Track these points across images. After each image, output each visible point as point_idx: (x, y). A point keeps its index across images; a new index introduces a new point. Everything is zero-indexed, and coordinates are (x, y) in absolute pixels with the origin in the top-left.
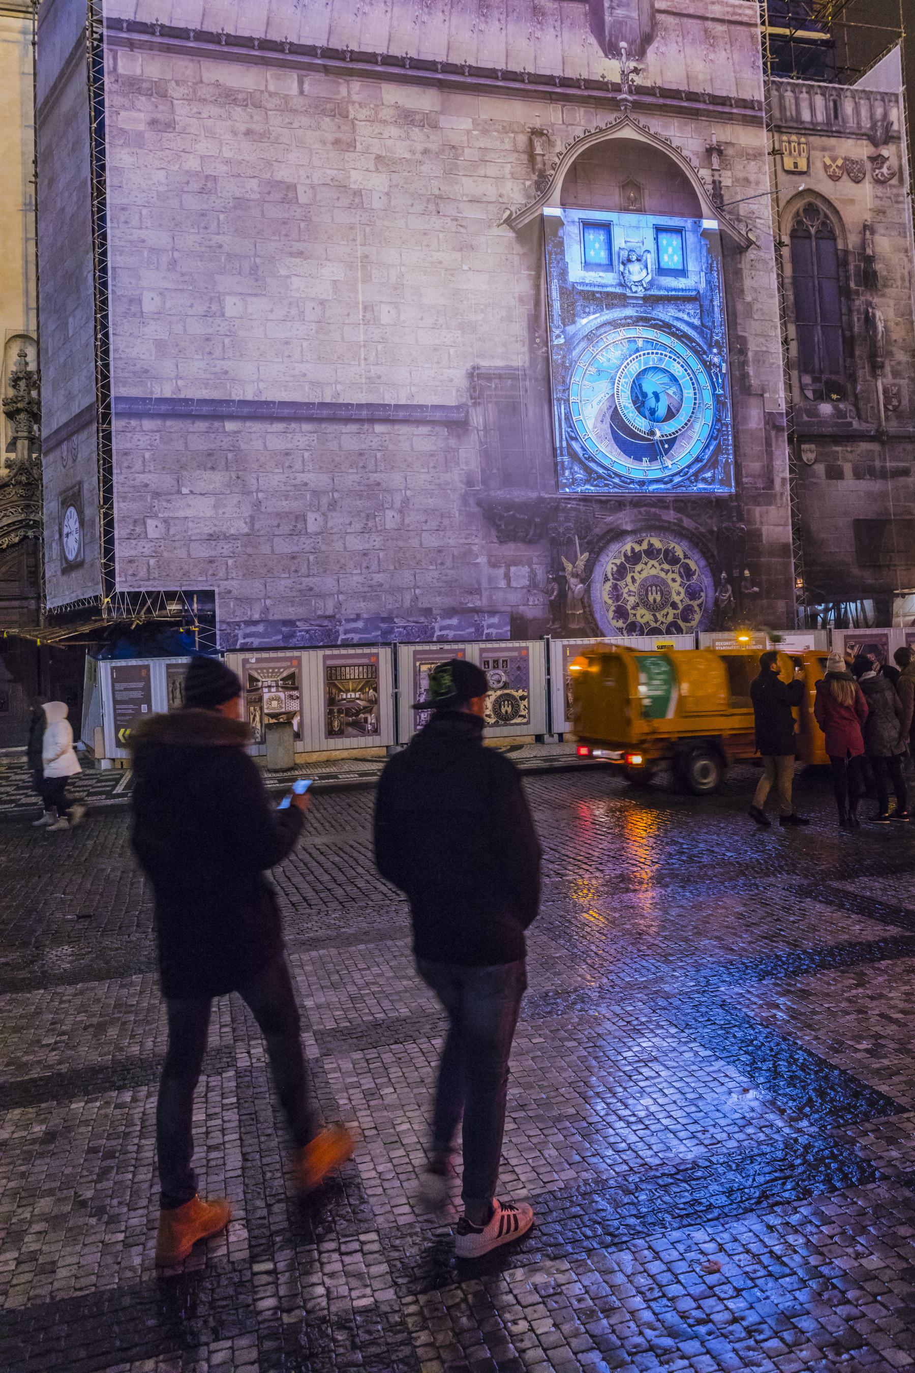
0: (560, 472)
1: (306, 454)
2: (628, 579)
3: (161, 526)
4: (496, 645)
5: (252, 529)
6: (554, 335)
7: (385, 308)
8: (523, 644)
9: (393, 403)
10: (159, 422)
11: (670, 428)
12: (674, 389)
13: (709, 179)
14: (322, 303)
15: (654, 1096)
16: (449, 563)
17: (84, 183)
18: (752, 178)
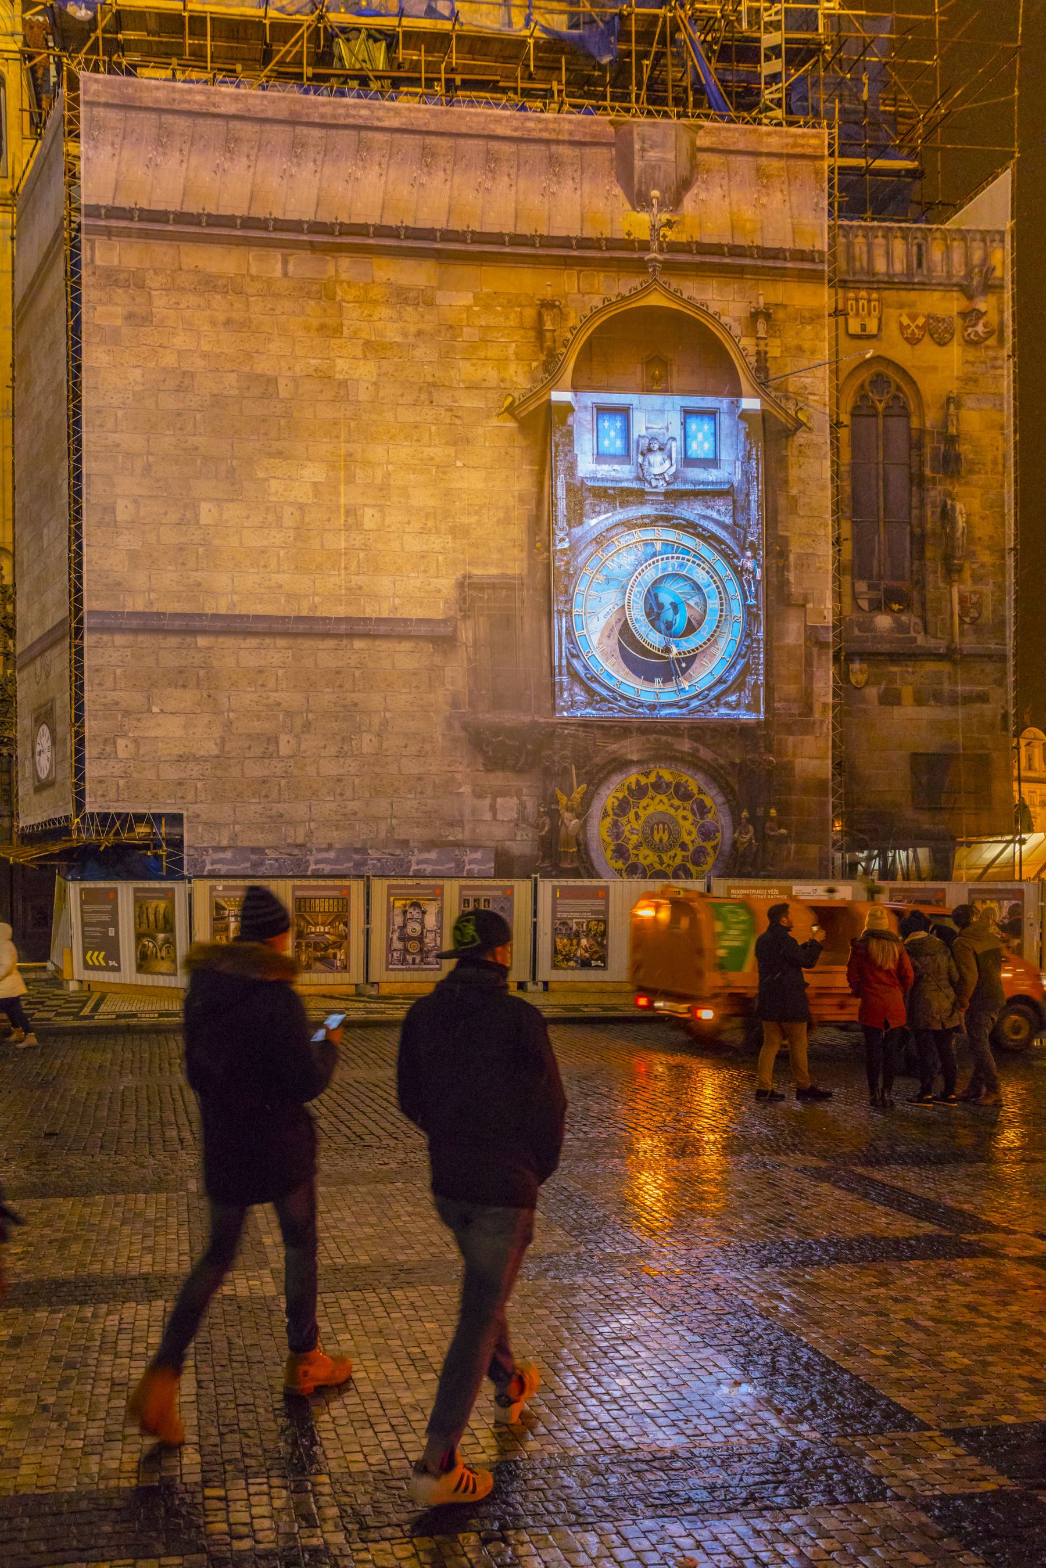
0: (557, 693)
1: (280, 672)
2: (631, 815)
3: (131, 746)
4: (478, 883)
5: (222, 750)
6: (558, 538)
7: (369, 512)
8: (506, 883)
9: (374, 616)
10: (131, 637)
11: (689, 644)
12: (696, 599)
13: (752, 350)
14: (301, 507)
16: (429, 791)
17: (60, 385)
18: (806, 345)
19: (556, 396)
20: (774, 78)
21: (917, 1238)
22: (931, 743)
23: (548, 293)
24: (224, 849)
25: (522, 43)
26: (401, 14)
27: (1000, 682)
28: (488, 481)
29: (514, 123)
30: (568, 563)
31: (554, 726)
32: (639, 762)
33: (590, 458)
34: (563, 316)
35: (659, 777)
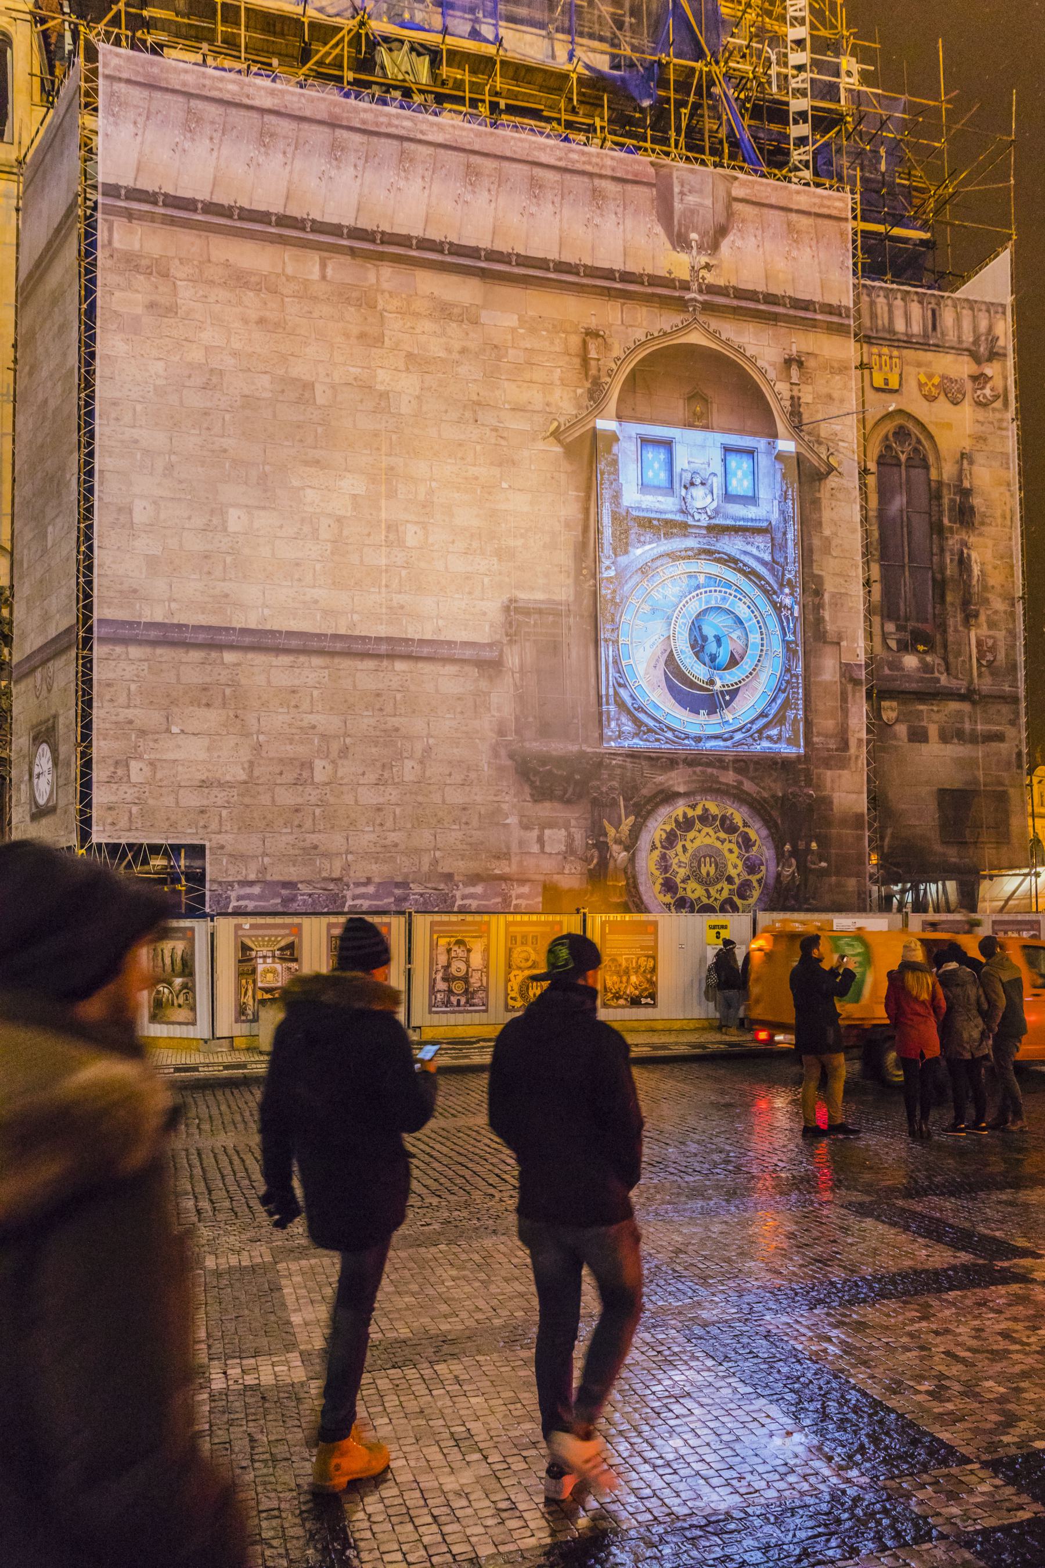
0: (605, 723)
1: (316, 693)
5: (251, 777)
6: (604, 566)
10: (148, 650)
11: (732, 677)
12: (738, 633)
13: (786, 395)
15: (685, 1437)
16: (475, 822)
19: (601, 424)
20: (802, 141)
21: (954, 1268)
22: (954, 779)
23: (593, 323)
24: (251, 884)
25: (565, 77)
26: (445, 31)
27: (1013, 723)
28: (536, 504)
29: (558, 153)
30: (614, 591)
31: (602, 756)
32: (686, 795)
33: (635, 488)
34: (607, 346)
35: (705, 810)
